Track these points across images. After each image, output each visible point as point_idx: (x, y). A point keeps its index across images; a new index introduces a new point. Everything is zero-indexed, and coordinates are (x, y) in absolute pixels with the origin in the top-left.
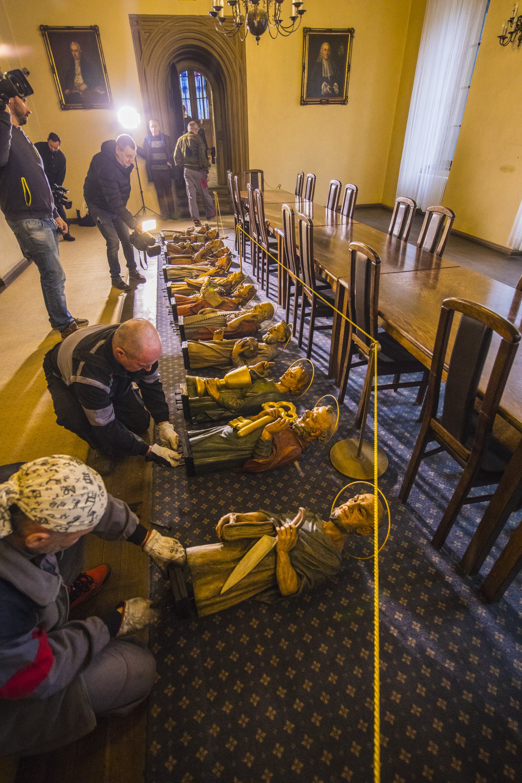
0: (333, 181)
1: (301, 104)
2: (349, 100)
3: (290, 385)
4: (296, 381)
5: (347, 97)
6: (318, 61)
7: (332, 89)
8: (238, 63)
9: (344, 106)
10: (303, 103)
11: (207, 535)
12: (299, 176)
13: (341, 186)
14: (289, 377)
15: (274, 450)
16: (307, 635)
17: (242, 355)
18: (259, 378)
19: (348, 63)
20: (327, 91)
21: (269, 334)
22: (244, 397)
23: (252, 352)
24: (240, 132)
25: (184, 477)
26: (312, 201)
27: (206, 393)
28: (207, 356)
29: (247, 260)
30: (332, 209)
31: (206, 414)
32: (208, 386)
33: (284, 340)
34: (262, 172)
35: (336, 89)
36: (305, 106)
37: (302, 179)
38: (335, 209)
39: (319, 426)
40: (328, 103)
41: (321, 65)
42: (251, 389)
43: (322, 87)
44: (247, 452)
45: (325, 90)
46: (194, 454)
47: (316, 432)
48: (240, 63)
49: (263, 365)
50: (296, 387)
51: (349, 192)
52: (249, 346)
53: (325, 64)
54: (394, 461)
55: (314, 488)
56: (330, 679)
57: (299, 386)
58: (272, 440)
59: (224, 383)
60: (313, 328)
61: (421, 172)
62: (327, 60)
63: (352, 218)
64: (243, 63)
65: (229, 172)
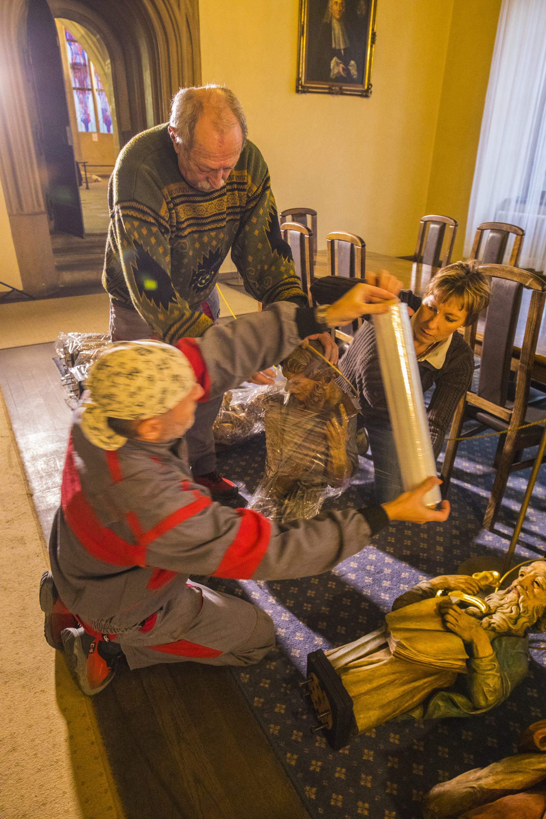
1: (298, 91)
2: (373, 89)
5: (370, 84)
6: (325, 21)
8: (183, 7)
9: (365, 100)
10: (301, 89)
19: (373, 30)
20: (339, 73)
36: (303, 95)
40: (341, 93)
41: (329, 27)
43: (332, 65)
45: (336, 71)
48: (187, 9)
53: (337, 28)
62: (339, 20)
64: (193, 7)
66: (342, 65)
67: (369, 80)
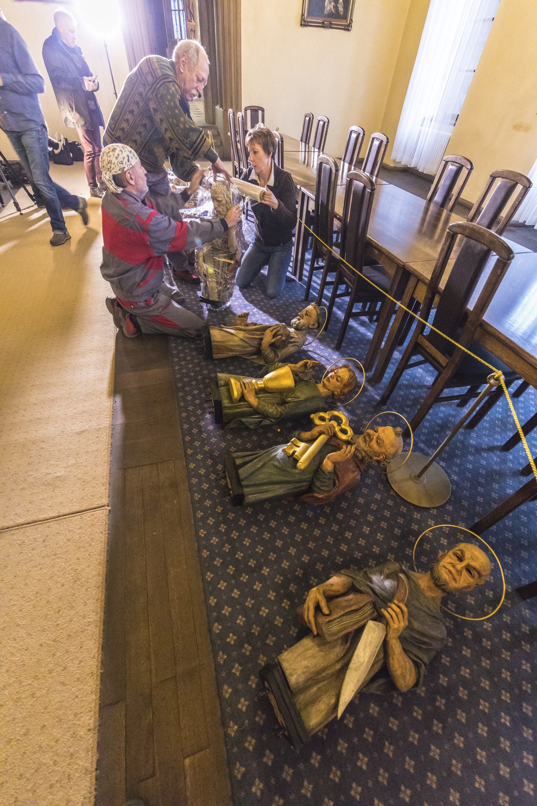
0: (355, 128)
2: (353, 24)
3: (334, 389)
4: (342, 386)
5: (351, 20)
7: (336, 7)
9: (347, 32)
10: (304, 24)
11: (271, 592)
12: (307, 118)
13: (364, 135)
14: (335, 380)
15: (337, 482)
16: (412, 733)
17: (272, 346)
18: (301, 380)
20: (331, 9)
21: (299, 320)
22: (283, 403)
23: (284, 341)
24: (233, 56)
25: (229, 507)
26: (323, 150)
27: (242, 398)
28: (231, 346)
29: (249, 218)
30: (350, 163)
31: (242, 423)
32: (245, 391)
33: (316, 326)
34: (263, 110)
35: (341, 9)
36: (305, 28)
37: (310, 122)
38: (354, 164)
39: (383, 450)
40: (330, 26)
42: (293, 394)
43: (326, 3)
44: (304, 484)
46: (246, 490)
47: (379, 456)
49: (305, 365)
50: (341, 392)
51: (376, 143)
52: (282, 335)
54: (454, 480)
55: (378, 520)
56: (451, 798)
57: (346, 391)
58: (334, 469)
59: (263, 386)
60: (349, 315)
61: (422, 125)
63: (377, 176)
65: (218, 107)
66: (333, 3)
67: (351, 16)
